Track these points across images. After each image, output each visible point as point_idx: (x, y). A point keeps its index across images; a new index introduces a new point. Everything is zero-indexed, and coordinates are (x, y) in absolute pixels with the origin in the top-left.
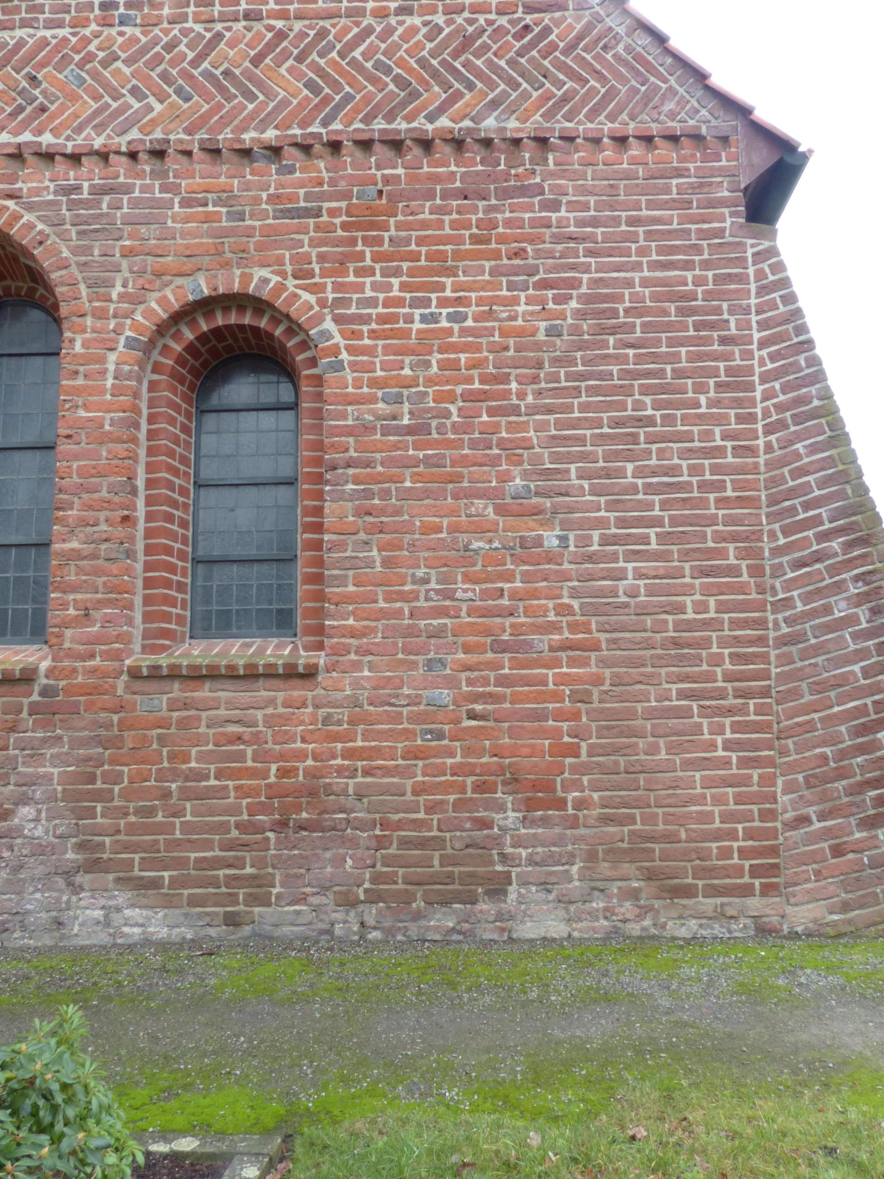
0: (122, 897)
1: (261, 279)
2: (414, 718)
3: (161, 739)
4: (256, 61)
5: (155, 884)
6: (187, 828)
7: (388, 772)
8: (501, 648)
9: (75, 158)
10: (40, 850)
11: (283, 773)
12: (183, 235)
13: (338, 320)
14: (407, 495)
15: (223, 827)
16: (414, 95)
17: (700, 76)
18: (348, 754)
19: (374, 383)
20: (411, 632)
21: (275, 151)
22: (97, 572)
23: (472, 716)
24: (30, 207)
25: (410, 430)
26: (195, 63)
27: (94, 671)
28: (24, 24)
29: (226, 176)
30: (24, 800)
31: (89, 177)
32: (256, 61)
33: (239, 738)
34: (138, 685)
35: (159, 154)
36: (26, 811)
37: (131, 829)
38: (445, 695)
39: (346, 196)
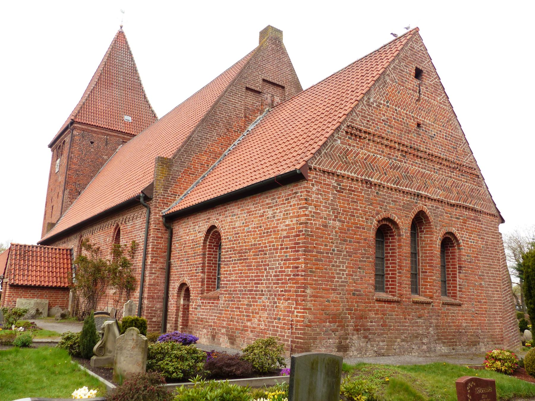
0: (442, 345)
1: (454, 230)
2: (471, 314)
3: (445, 316)
4: (451, 186)
5: (444, 343)
6: (449, 332)
7: (469, 323)
8: (479, 302)
9: (432, 200)
10: (433, 336)
11: (459, 323)
12: (446, 219)
13: (462, 240)
14: (470, 274)
15: (452, 332)
16: (468, 199)
17: (495, 205)
18: (465, 319)
19: (466, 253)
20: (470, 298)
21: (454, 205)
22: (437, 283)
23: (476, 314)
24: (428, 209)
25: (470, 262)
26: (445, 184)
27: (438, 302)
28: (425, 169)
29: (449, 209)
30: (430, 327)
31: (435, 204)
32: (451, 186)
33: (454, 316)
34: (444, 306)
35: (442, 202)
36: (431, 328)
37: (443, 332)
38: (474, 309)
39: (462, 216)
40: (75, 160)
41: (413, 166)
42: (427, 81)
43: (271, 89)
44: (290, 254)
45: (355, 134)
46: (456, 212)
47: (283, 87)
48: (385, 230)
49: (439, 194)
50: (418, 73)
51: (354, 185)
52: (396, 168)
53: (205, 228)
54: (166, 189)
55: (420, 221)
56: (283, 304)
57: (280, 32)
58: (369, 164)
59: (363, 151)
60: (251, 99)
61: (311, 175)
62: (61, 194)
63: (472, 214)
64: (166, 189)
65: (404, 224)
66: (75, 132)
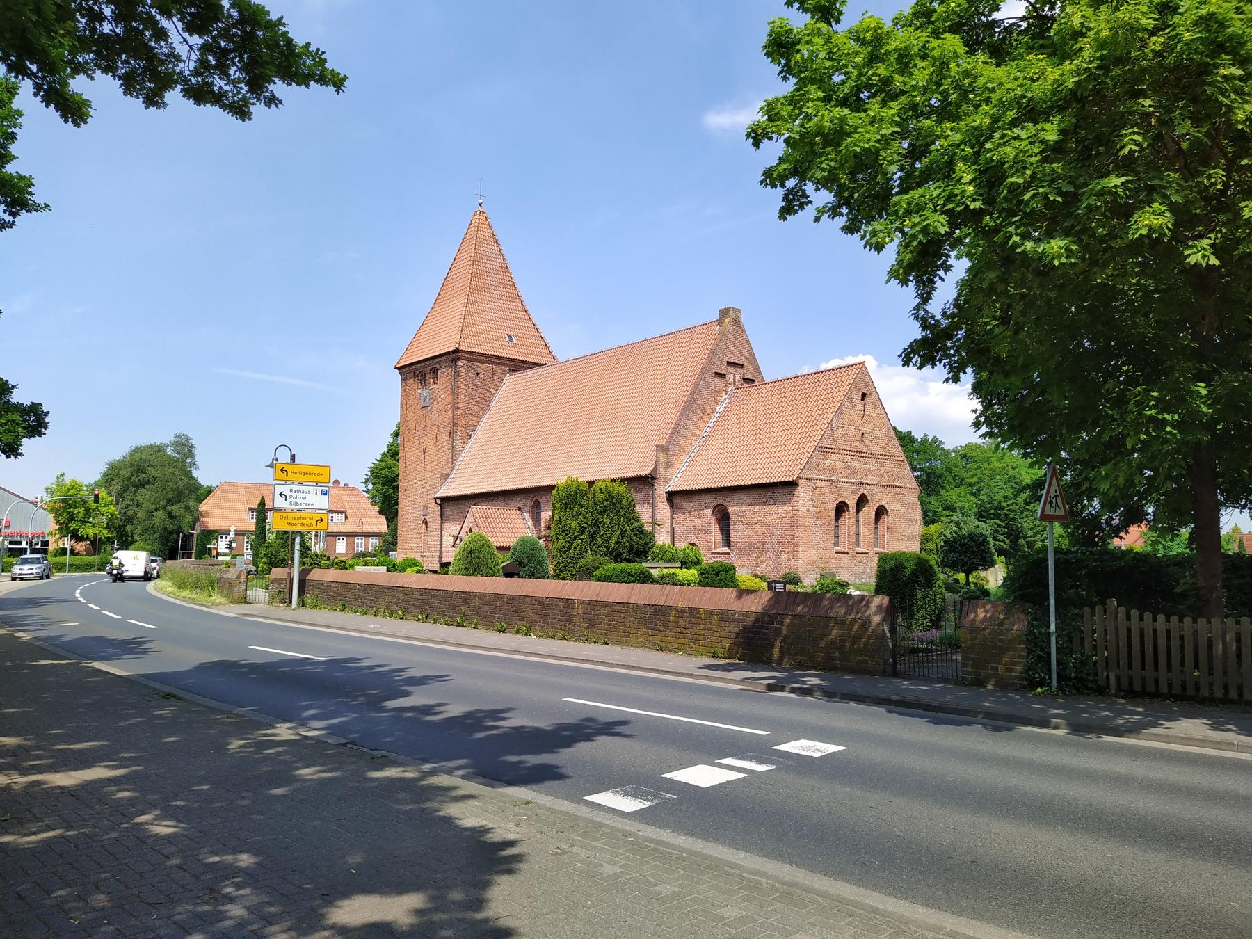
1: (883, 503)
29: (881, 489)
40: (462, 398)
41: (857, 464)
42: (868, 400)
43: (733, 369)
44: (788, 527)
45: (823, 450)
46: (887, 490)
47: (742, 366)
48: (841, 508)
49: (877, 480)
50: (864, 396)
51: (824, 484)
52: (847, 467)
53: (713, 504)
54: (666, 470)
55: (862, 501)
56: (784, 556)
57: (739, 311)
58: (832, 470)
59: (826, 461)
60: (718, 380)
61: (801, 482)
62: (443, 436)
63: (898, 490)
64: (666, 470)
65: (852, 504)
66: (460, 363)
